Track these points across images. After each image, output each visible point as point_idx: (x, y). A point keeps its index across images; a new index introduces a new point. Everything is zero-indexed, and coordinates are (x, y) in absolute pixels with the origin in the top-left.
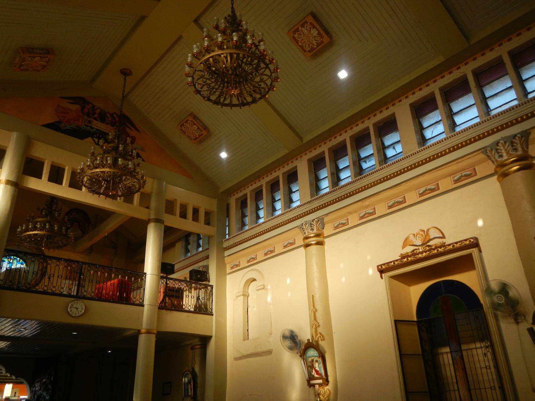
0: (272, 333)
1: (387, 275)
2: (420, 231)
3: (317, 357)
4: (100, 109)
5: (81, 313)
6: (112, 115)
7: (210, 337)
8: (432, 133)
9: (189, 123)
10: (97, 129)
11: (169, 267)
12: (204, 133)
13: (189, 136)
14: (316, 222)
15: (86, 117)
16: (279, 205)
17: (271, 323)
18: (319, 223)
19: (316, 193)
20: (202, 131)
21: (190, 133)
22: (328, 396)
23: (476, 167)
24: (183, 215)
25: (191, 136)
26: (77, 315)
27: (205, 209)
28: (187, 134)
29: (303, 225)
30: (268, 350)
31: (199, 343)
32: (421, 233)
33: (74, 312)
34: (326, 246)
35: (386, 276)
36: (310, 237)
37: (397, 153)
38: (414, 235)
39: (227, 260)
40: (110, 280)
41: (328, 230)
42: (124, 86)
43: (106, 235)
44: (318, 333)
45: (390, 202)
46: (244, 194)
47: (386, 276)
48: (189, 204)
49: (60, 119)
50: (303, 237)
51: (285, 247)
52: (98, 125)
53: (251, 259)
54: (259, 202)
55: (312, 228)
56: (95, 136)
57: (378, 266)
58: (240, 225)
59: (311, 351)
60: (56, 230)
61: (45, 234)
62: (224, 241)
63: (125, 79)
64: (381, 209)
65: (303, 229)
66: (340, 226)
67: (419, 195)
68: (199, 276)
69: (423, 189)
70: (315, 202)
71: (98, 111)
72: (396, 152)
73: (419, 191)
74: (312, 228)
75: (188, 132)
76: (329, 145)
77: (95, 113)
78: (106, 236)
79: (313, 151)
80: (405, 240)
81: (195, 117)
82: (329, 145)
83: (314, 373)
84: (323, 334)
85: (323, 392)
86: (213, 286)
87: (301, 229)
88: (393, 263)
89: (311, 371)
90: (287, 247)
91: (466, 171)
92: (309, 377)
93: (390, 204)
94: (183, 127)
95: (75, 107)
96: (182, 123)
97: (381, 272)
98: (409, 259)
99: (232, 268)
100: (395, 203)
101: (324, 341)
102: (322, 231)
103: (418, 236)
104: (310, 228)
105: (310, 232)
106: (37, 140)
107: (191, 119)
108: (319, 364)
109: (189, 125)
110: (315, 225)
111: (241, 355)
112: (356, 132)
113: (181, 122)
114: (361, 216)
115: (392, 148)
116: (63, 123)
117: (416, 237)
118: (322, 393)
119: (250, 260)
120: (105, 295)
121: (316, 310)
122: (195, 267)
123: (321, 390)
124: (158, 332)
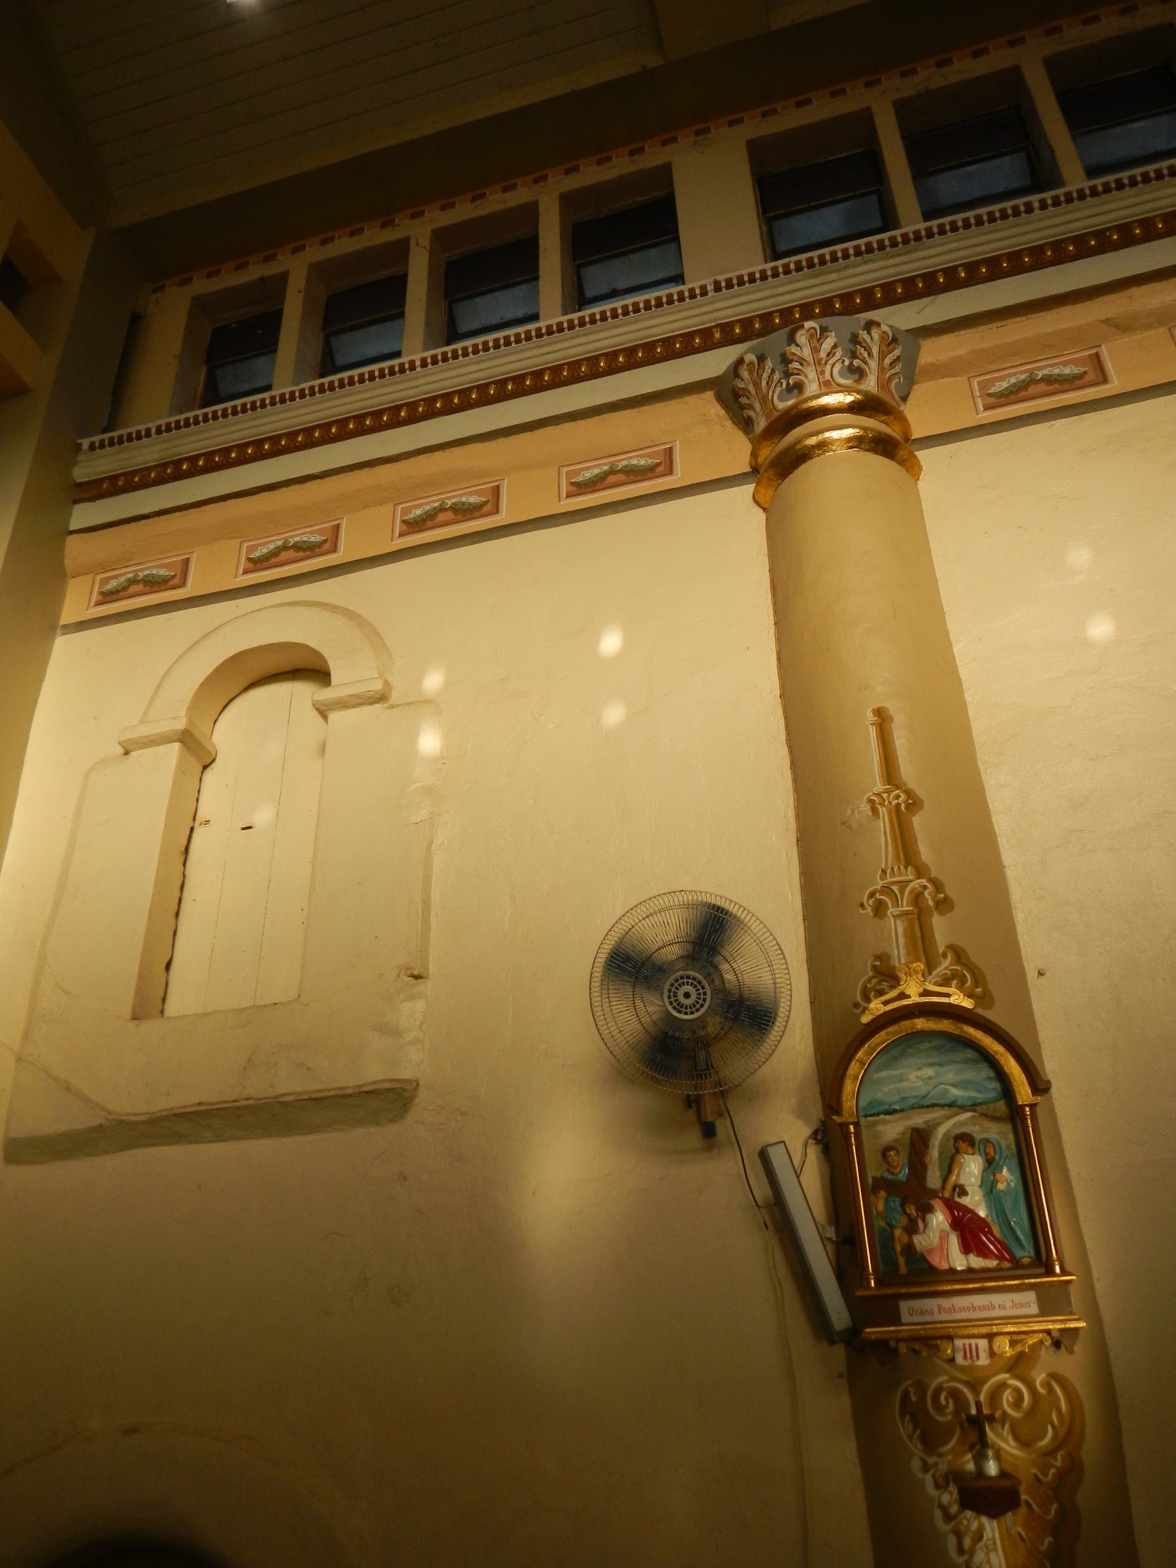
0: (427, 969)
3: (969, 1114)
18: (897, 353)
22: (1069, 1432)
34: (926, 485)
39: (76, 550)
44: (941, 949)
46: (262, 279)
54: (346, 338)
55: (856, 362)
65: (785, 360)
74: (856, 362)
84: (975, 957)
85: (1017, 1403)
87: (769, 364)
90: (599, 486)
104: (847, 363)
105: (842, 381)
108: (990, 1164)
110: (875, 350)
111: (86, 1120)
119: (275, 553)
121: (914, 804)
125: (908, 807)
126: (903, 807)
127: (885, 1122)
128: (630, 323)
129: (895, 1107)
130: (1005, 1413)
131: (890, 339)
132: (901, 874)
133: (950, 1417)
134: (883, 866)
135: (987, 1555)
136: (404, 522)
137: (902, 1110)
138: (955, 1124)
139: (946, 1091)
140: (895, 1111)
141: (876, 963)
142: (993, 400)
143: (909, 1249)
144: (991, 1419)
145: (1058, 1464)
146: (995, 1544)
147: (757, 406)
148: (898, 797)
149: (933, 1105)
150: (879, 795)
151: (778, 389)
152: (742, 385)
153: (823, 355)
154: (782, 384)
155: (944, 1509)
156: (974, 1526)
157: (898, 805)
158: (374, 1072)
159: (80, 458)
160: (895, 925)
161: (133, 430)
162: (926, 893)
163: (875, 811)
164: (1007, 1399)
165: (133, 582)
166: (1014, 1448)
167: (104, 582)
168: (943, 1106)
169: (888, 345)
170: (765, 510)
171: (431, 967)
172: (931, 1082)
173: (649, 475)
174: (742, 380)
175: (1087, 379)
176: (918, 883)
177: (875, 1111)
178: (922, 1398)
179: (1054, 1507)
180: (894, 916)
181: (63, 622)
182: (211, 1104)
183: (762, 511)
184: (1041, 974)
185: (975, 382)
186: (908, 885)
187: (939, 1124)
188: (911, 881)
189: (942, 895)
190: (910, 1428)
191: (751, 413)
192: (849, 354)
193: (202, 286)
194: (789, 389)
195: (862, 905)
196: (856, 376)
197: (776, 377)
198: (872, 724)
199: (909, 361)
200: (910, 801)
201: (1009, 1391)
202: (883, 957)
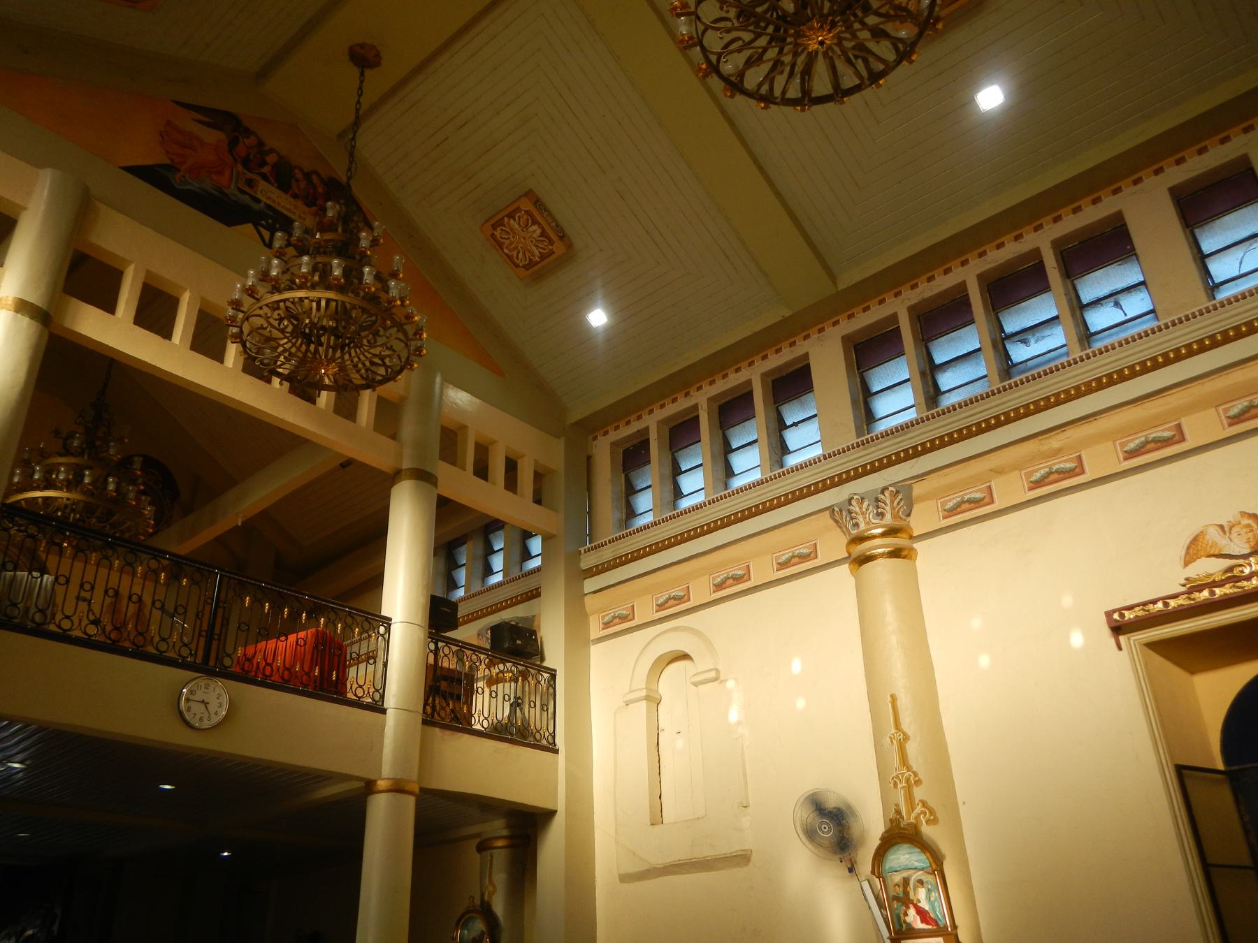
1: (1134, 638)
2: (1242, 516)
4: (278, 155)
5: (215, 720)
6: (307, 176)
7: (551, 814)
8: (1241, 263)
9: (519, 217)
10: (268, 207)
11: (445, 609)
12: (559, 248)
13: (510, 258)
14: (891, 495)
15: (240, 167)
16: (644, 502)
17: (745, 774)
18: (900, 497)
19: (867, 425)
20: (551, 242)
21: (516, 248)
24: (482, 471)
25: (518, 256)
26: (206, 724)
27: (536, 461)
28: (506, 251)
29: (854, 502)
30: (739, 853)
31: (505, 833)
32: (1246, 521)
33: (195, 714)
34: (920, 562)
35: (1134, 641)
36: (874, 537)
37: (1129, 317)
38: (1222, 527)
40: (294, 630)
41: (920, 520)
42: (360, 91)
43: (240, 524)
45: (1132, 441)
46: (638, 431)
47: (1134, 641)
48: (494, 442)
49: (172, 160)
50: (844, 540)
51: (783, 565)
52: (269, 194)
53: (670, 599)
55: (880, 510)
56: (263, 222)
57: (1109, 614)
58: (622, 513)
59: (900, 852)
60: (111, 491)
61: (79, 501)
62: (583, 552)
63: (362, 74)
64: (1099, 460)
65: (850, 512)
66: (964, 506)
67: (1230, 420)
68: (519, 642)
69: (1244, 403)
70: (882, 443)
71: (271, 159)
72: (1126, 315)
73: (1226, 411)
74: (880, 510)
75: (511, 244)
76: (909, 299)
77: (264, 163)
78: (237, 526)
79: (858, 316)
81: (537, 202)
82: (909, 299)
83: (912, 917)
84: (931, 804)
86: (555, 671)
87: (844, 513)
88: (1160, 605)
89: (902, 912)
90: (789, 565)
92: (896, 929)
93: (1132, 446)
94: (498, 229)
95: (212, 137)
96: (497, 218)
97: (1118, 629)
98: (1218, 591)
99: (607, 625)
100: (1147, 442)
101: (936, 826)
102: (905, 520)
103: (1235, 530)
104: (875, 512)
105: (874, 521)
106: (106, 204)
107: (526, 205)
108: (929, 891)
109: (520, 226)
110: (888, 502)
112: (997, 264)
113: (494, 216)
114: (1034, 478)
115: (1112, 304)
116: (179, 171)
117: (1228, 533)
119: (666, 602)
120: (281, 671)
121: (906, 738)
122: (506, 615)
124: (422, 790)
128: (791, 478)
136: (714, 585)
142: (946, 513)
143: (905, 922)
148: (900, 735)
149: (909, 869)
150: (893, 734)
153: (864, 510)
157: (900, 739)
158: (735, 848)
159: (582, 557)
161: (600, 542)
165: (614, 617)
167: (603, 617)
168: (912, 869)
171: (750, 802)
173: (808, 559)
181: (591, 639)
182: (683, 860)
184: (964, 803)
187: (911, 876)
193: (614, 436)
196: (881, 517)
202: (897, 805)
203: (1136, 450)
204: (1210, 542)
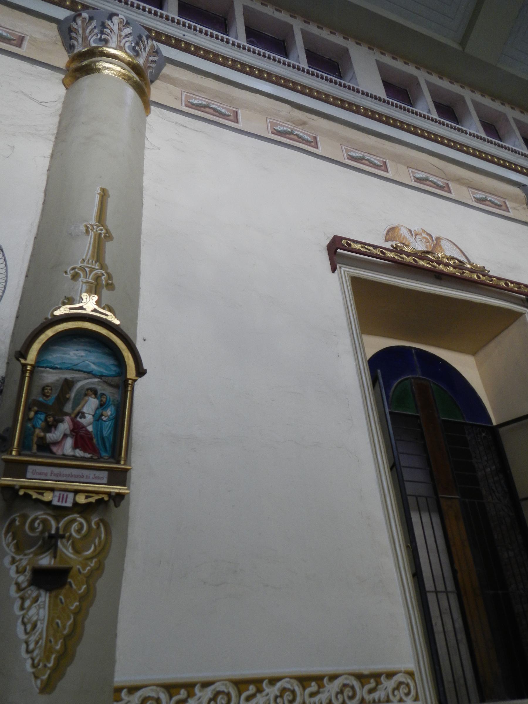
3: (97, 380)
23: (507, 202)
29: (115, 19)
32: (424, 235)
35: (344, 271)
38: (410, 231)
55: (137, 48)
65: (103, 26)
74: (137, 48)
80: (390, 229)
85: (79, 531)
87: (94, 23)
91: (493, 198)
100: (363, 158)
104: (133, 45)
105: (128, 51)
108: (102, 405)
110: (147, 49)
114: (278, 128)
118: (74, 534)
121: (109, 237)
123: (74, 521)
125: (105, 236)
126: (103, 236)
127: (49, 373)
129: (56, 366)
130: (71, 535)
131: (155, 50)
132: (92, 264)
133: (37, 534)
134: (84, 257)
135: (38, 610)
137: (61, 369)
138: (89, 382)
139: (89, 365)
140: (56, 368)
141: (65, 301)
142: (190, 105)
144: (62, 537)
145: (93, 565)
146: (44, 605)
147: (80, 40)
148: (101, 230)
149: (79, 371)
150: (92, 225)
151: (95, 37)
152: (76, 27)
154: (98, 35)
155: (18, 584)
156: (35, 594)
157: (100, 234)
160: (82, 285)
162: (103, 278)
163: (87, 232)
164: (75, 527)
166: (71, 553)
168: (84, 372)
169: (154, 52)
170: (67, 88)
172: (81, 358)
174: (77, 24)
175: (230, 118)
176: (100, 272)
177: (45, 365)
178: (23, 523)
179: (84, 587)
180: (83, 282)
183: (65, 88)
185: (184, 94)
186: (95, 271)
187: (79, 381)
188: (97, 269)
189: (111, 282)
190: (10, 539)
191: (76, 43)
192: (135, 42)
194: (101, 40)
195: (66, 272)
197: (96, 31)
198: (98, 194)
199: (159, 69)
200: (107, 235)
201: (77, 523)
203: (356, 158)
204: (403, 235)
